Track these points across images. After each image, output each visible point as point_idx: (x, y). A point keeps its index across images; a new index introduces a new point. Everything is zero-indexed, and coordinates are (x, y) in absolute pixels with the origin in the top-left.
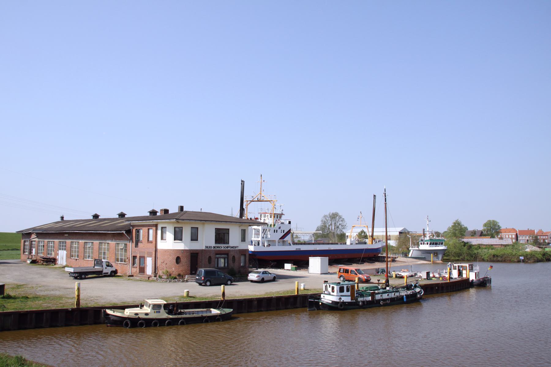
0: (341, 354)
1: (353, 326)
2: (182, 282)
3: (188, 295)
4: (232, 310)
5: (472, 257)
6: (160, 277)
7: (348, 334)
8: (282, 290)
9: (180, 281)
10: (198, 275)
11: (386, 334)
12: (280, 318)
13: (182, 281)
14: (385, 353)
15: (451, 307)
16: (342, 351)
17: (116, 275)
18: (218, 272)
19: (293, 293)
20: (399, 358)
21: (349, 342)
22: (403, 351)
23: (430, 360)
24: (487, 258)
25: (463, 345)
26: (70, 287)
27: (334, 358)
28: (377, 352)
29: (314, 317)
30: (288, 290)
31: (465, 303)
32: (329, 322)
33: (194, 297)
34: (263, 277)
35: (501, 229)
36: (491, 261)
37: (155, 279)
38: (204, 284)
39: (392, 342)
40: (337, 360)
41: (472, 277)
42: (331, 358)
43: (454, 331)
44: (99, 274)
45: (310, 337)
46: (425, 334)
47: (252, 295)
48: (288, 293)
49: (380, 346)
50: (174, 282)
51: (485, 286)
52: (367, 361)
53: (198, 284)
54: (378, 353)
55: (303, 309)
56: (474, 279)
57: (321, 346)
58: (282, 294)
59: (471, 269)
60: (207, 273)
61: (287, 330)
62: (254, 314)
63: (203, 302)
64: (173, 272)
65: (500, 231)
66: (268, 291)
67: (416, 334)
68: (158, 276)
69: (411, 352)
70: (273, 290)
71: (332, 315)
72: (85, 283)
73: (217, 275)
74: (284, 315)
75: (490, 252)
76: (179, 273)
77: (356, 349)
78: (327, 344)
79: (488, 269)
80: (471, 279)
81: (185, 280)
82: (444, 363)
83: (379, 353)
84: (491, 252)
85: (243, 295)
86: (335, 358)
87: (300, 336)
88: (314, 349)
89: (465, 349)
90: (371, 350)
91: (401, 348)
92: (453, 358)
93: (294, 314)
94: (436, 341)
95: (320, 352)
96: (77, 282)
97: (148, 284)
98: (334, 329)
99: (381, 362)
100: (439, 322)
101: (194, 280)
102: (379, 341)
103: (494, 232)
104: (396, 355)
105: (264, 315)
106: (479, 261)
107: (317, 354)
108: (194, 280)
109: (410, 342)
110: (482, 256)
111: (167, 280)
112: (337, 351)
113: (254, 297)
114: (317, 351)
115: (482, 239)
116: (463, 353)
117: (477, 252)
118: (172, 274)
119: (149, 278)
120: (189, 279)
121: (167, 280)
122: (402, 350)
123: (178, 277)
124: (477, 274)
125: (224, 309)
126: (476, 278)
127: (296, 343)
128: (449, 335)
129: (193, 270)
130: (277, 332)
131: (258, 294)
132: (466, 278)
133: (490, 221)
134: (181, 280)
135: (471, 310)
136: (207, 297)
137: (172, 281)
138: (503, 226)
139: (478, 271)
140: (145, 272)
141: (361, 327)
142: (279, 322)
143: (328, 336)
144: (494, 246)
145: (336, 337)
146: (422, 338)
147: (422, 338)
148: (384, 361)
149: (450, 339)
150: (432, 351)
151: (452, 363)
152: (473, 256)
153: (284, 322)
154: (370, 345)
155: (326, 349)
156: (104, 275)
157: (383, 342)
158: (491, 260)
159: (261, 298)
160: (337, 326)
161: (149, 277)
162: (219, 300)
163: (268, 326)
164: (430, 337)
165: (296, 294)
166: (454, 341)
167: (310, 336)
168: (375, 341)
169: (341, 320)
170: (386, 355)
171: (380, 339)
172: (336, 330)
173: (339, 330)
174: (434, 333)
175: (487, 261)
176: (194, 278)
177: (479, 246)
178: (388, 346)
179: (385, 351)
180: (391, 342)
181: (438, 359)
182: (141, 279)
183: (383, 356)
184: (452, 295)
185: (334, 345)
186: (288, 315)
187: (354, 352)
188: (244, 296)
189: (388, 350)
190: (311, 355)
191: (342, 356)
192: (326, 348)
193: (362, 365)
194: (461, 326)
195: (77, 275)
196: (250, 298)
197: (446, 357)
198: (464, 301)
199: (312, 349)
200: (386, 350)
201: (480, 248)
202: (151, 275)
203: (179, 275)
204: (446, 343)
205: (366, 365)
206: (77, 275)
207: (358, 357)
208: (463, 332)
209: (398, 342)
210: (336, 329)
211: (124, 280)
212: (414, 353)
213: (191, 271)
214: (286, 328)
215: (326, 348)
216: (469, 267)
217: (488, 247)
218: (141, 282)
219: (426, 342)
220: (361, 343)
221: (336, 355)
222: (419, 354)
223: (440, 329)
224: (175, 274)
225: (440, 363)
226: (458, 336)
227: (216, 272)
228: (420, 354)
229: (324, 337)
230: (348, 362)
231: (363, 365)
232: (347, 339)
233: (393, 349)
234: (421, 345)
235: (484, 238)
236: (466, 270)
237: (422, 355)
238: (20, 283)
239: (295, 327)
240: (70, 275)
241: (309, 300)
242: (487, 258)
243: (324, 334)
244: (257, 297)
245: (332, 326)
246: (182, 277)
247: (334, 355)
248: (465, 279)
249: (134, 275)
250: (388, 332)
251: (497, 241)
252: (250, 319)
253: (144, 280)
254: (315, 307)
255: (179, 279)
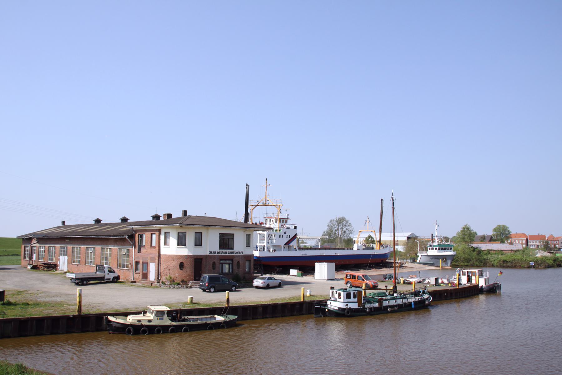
0: (348, 361)
1: (360, 333)
2: (186, 288)
3: (192, 302)
4: (236, 317)
5: (482, 262)
6: (164, 283)
7: (354, 341)
8: (288, 296)
9: (184, 287)
10: (202, 281)
11: (394, 341)
12: (286, 325)
13: (185, 287)
14: (393, 361)
15: (460, 314)
16: (349, 358)
17: (118, 281)
18: (222, 278)
19: (299, 300)
20: (407, 366)
21: (356, 349)
22: (411, 358)
23: (438, 367)
24: (497, 263)
25: (472, 352)
26: (71, 294)
27: (340, 366)
28: (385, 360)
29: (321, 323)
30: (294, 296)
31: (474, 309)
32: (336, 329)
33: (198, 304)
34: (268, 283)
35: (511, 234)
36: (501, 266)
37: (158, 285)
38: (208, 290)
39: (399, 350)
40: (343, 368)
41: (482, 283)
42: (338, 366)
43: (463, 338)
44: (101, 280)
45: (316, 344)
46: (433, 341)
47: (257, 302)
48: (294, 300)
49: (388, 354)
50: (177, 288)
51: (495, 293)
52: (374, 369)
53: (202, 290)
54: (385, 361)
55: (309, 315)
56: (484, 285)
57: (327, 353)
58: (287, 300)
59: (481, 275)
60: (211, 278)
61: (292, 337)
62: (259, 321)
63: (207, 308)
64: (176, 278)
65: (510, 236)
66: (274, 298)
67: (425, 341)
68: (161, 282)
69: (420, 360)
70: (278, 296)
71: (339, 321)
72: (86, 290)
73: (221, 281)
74: (290, 322)
75: (500, 257)
76: (183, 279)
77: (364, 357)
78: (334, 351)
79: (498, 275)
80: (480, 285)
81: (189, 286)
82: (453, 371)
83: (386, 361)
84: (501, 257)
85: (248, 302)
86: (342, 366)
87: (306, 344)
88: (320, 357)
89: (475, 356)
90: (379, 358)
91: (409, 356)
92: (462, 366)
93: (299, 321)
94: (445, 348)
95: (326, 359)
96: (78, 288)
97: (151, 290)
98: (340, 336)
99: (389, 370)
100: (448, 329)
101: (198, 286)
102: (386, 348)
103: (504, 237)
104: (404, 362)
105: (270, 322)
106: (489, 267)
107: (323, 361)
108: (198, 286)
109: (419, 349)
110: (491, 262)
111: (170, 286)
112: (344, 359)
113: (259, 303)
114: (323, 358)
115: (491, 244)
116: (472, 360)
117: (487, 258)
118: (175, 280)
119: (152, 284)
120: (193, 285)
121: (170, 286)
122: (410, 357)
123: (181, 284)
124: (486, 280)
125: (229, 316)
126: (485, 284)
127: (302, 351)
128: (458, 343)
129: (197, 276)
130: (282, 339)
131: (263, 300)
132: (475, 284)
133: (500, 225)
134: (184, 286)
135: (480, 317)
136: (211, 303)
137: (176, 287)
138: (513, 231)
139: (488, 277)
140: (148, 278)
141: (368, 335)
142: (284, 329)
143: (335, 343)
144: (503, 251)
145: (343, 344)
146: (431, 346)
147: (431, 346)
148: (391, 369)
149: (459, 346)
150: (441, 359)
151: (461, 371)
152: (483, 261)
153: (289, 329)
154: (377, 353)
155: (333, 357)
156: (106, 281)
157: (391, 350)
158: (501, 265)
159: (266, 304)
160: (344, 333)
161: (152, 283)
162: (223, 307)
163: (273, 333)
164: (438, 345)
165: (302, 300)
166: (463, 348)
167: (316, 343)
168: (382, 348)
169: (348, 327)
170: (394, 363)
171: (388, 347)
172: (343, 337)
173: (346, 338)
174: (442, 340)
175: (497, 267)
176: (198, 284)
177: (489, 252)
178: (396, 354)
179: (393, 358)
180: (399, 349)
181: (447, 366)
182: (144, 285)
183: (391, 364)
184: (461, 301)
185: (340, 353)
186: (293, 322)
187: (361, 360)
188: (249, 303)
189: (396, 358)
190: (317, 363)
191: (348, 364)
192: (332, 355)
193: (369, 373)
194: (470, 333)
195: (78, 281)
196: (255, 304)
197: (455, 365)
198: (473, 308)
199: (318, 357)
200: (394, 358)
201: (489, 253)
202: (154, 281)
203: (183, 281)
204: (455, 350)
205: (373, 373)
206: (78, 281)
207: (365, 364)
208: (472, 339)
209: (406, 349)
210: (343, 336)
211: (127, 286)
212: (423, 361)
213: (195, 277)
214: (292, 335)
215: (332, 355)
216: (479, 273)
217: (498, 252)
218: (143, 288)
219: (435, 349)
220: (368, 350)
221: (343, 363)
222: (427, 361)
223: (448, 337)
224: (178, 280)
225: (449, 371)
226: (467, 344)
227: (221, 278)
228: (428, 361)
229: (331, 345)
230: (355, 369)
231: (370, 373)
232: (354, 347)
233: (401, 356)
234: (430, 352)
235: (494, 243)
236: (476, 275)
237: (431, 362)
238: (20, 289)
239: (300, 334)
240: (71, 281)
241: (315, 306)
242: (497, 263)
243: (331, 341)
244: (262, 304)
245: (338, 334)
246: (186, 283)
247: (340, 363)
248: (474, 285)
249: (137, 281)
250: (395, 339)
251: (507, 246)
252: (255, 326)
253: (147, 286)
254: (321, 313)
255: (182, 286)
